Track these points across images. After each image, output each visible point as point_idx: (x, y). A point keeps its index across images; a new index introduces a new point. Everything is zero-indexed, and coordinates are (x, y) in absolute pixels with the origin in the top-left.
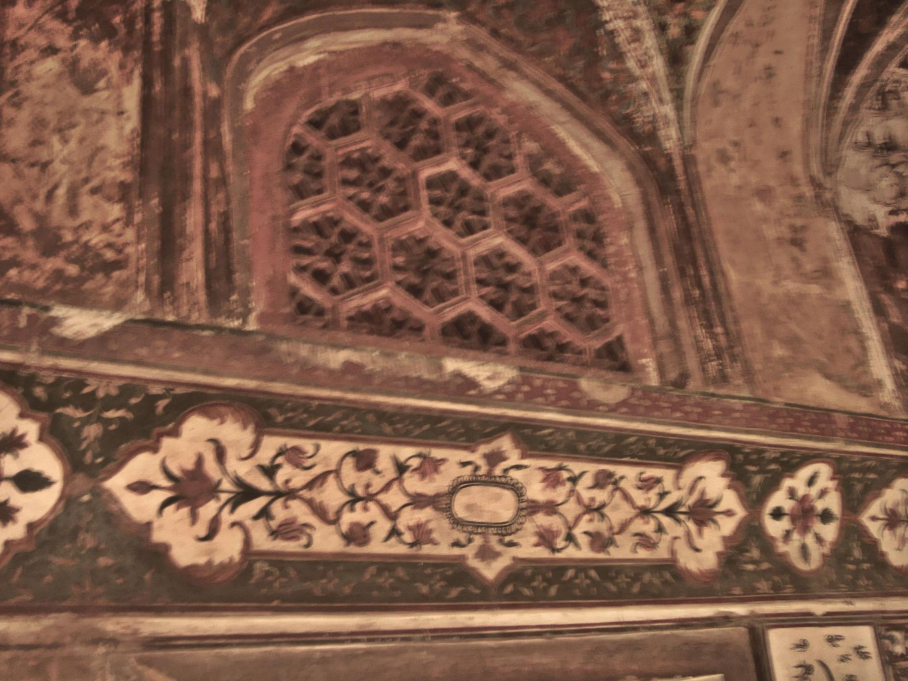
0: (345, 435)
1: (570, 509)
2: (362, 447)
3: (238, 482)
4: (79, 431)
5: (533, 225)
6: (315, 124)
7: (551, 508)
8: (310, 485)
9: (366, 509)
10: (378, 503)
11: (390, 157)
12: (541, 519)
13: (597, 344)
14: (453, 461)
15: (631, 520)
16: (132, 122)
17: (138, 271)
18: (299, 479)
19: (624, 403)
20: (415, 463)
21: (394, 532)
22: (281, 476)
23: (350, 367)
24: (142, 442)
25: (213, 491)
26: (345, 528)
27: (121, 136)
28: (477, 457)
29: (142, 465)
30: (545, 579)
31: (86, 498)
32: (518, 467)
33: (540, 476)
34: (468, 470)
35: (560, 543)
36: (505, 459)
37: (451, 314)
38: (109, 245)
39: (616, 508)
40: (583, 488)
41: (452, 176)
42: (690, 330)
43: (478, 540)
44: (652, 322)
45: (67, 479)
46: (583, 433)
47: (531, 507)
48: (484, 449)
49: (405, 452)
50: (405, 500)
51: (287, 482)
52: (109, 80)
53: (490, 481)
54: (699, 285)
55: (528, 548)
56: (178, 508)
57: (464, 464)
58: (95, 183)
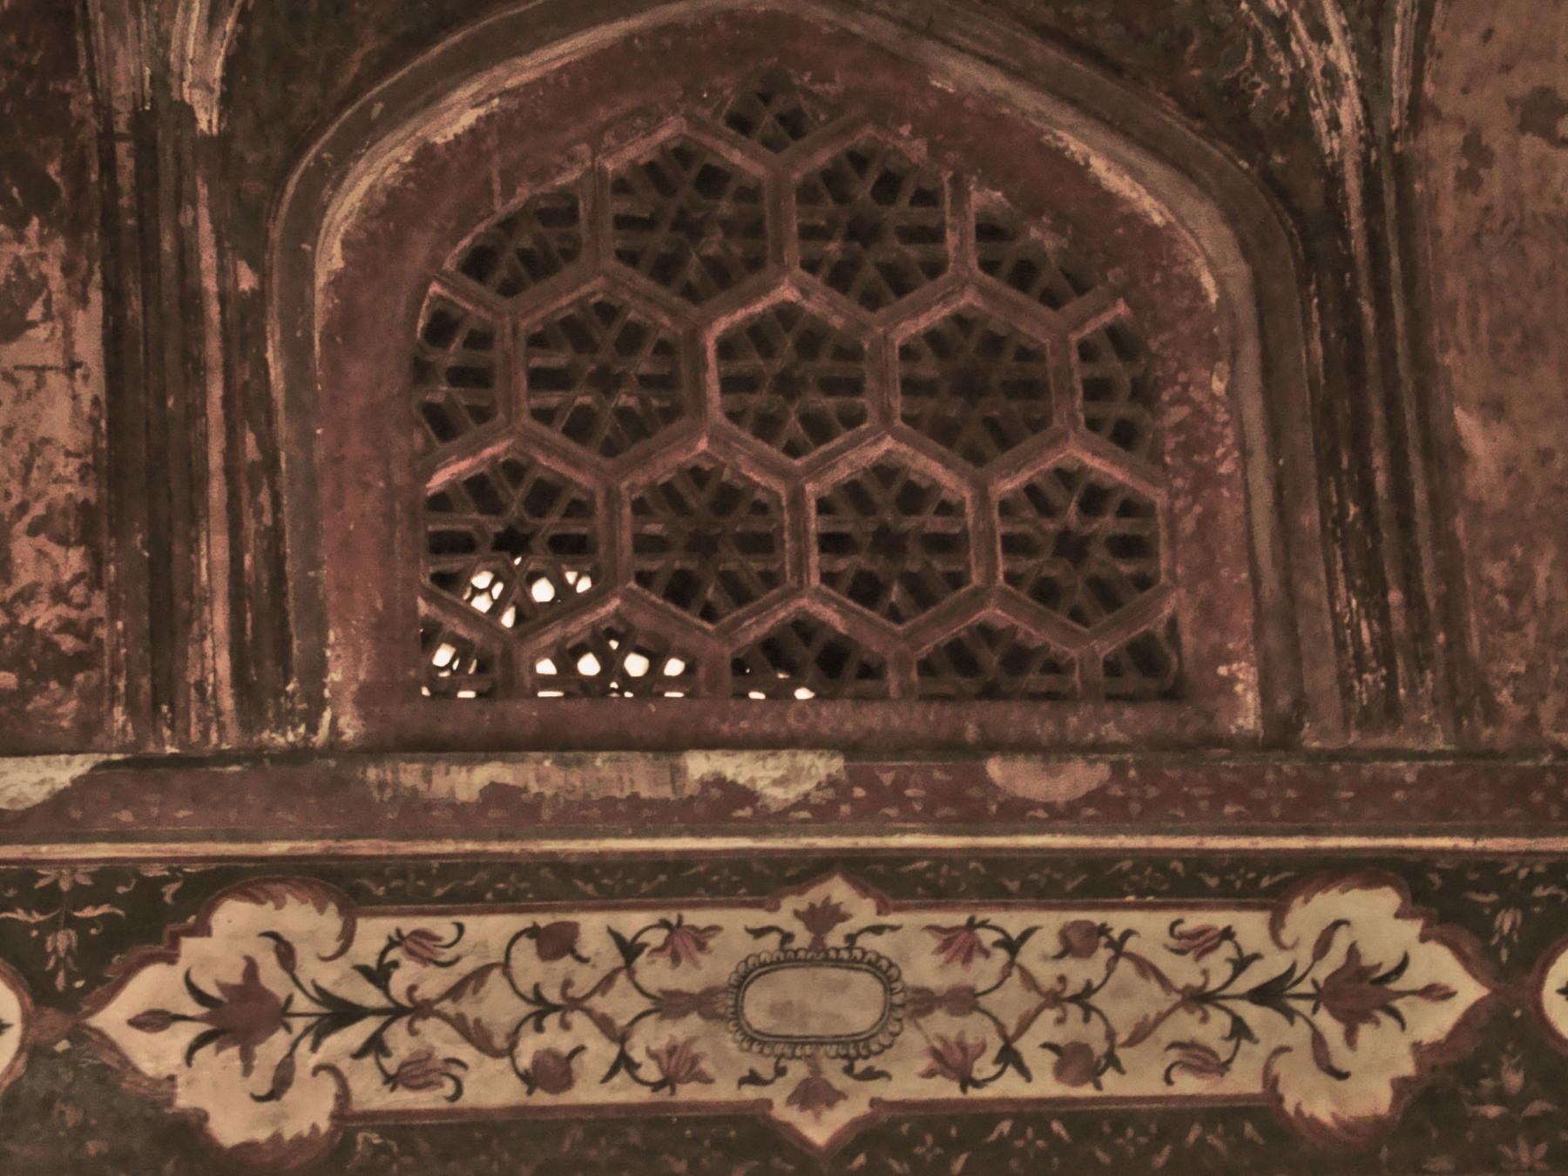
0: (507, 903)
1: (1011, 1001)
2: (544, 920)
3: (324, 996)
4: (41, 941)
5: (982, 393)
6: (478, 264)
7: (964, 1000)
8: (454, 993)
9: (565, 1026)
10: (589, 1012)
11: (649, 305)
12: (942, 1024)
13: (1105, 647)
14: (734, 928)
15: (1161, 1018)
16: (92, 388)
17: (115, 671)
18: (433, 983)
19: (1091, 798)
20: (656, 938)
21: (624, 1063)
22: (399, 983)
23: (496, 793)
24: (147, 949)
25: (280, 1015)
26: (525, 1062)
27: (76, 412)
28: (785, 915)
29: (151, 985)
30: (943, 1140)
31: (63, 1046)
32: (877, 930)
33: (932, 942)
34: (772, 941)
35: (984, 1067)
36: (845, 917)
37: (755, 630)
38: (67, 626)
39: (1123, 992)
40: (1038, 957)
41: (786, 314)
42: (1332, 599)
43: (798, 1071)
44: (1256, 580)
45: (27, 1019)
46: (999, 862)
47: (913, 1001)
48: (790, 904)
49: (632, 922)
50: (644, 1004)
51: (412, 989)
52: (47, 303)
53: (820, 957)
54: (1365, 493)
55: (910, 1080)
56: (219, 1049)
57: (758, 933)
58: (38, 509)
